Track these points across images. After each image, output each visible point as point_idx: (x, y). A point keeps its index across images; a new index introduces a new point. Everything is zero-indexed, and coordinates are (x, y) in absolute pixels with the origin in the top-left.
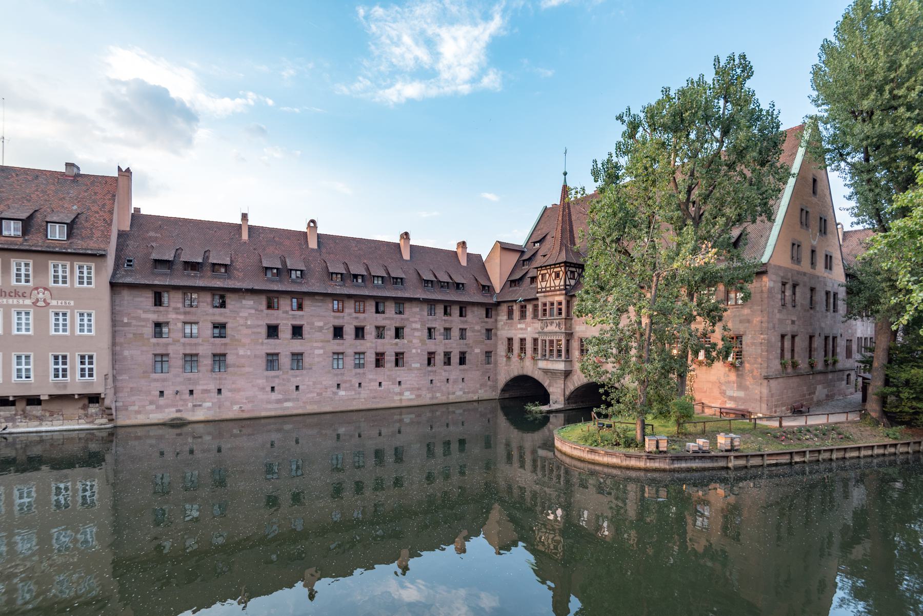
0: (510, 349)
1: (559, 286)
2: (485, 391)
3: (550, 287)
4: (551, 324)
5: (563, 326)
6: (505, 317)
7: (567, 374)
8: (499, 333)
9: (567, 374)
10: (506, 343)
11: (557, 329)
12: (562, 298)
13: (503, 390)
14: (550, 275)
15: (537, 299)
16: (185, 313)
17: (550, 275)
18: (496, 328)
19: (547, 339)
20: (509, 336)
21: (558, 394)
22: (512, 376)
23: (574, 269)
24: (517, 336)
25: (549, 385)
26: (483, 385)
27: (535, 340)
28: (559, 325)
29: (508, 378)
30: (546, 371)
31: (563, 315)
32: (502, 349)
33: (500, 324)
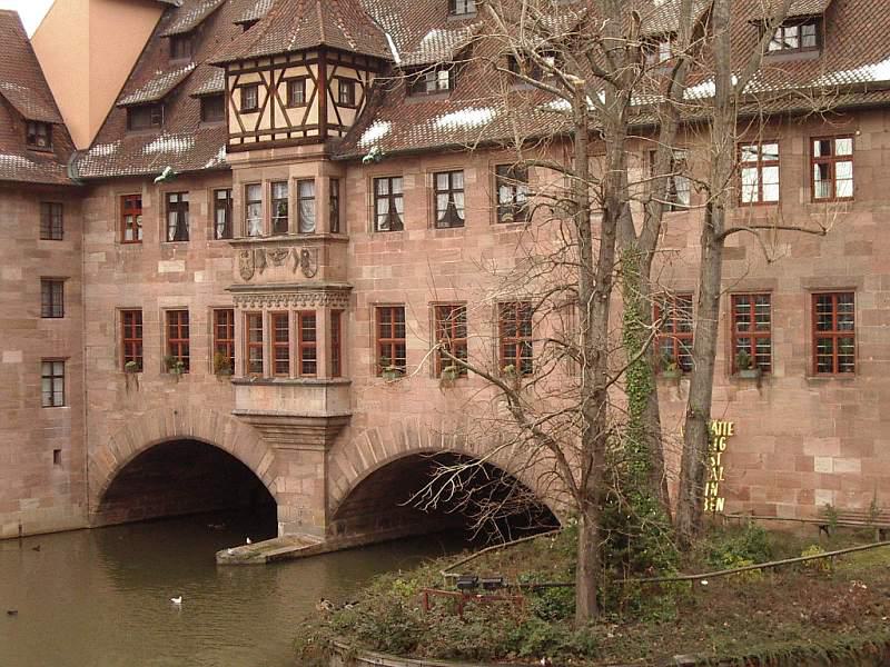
0: (132, 352)
1: (304, 128)
2: (46, 502)
3: (273, 131)
4: (278, 259)
5: (318, 268)
6: (111, 237)
7: (335, 429)
8: (91, 293)
9: (335, 429)
10: (116, 326)
11: (298, 277)
12: (313, 169)
13: (111, 496)
14: (272, 90)
17: (272, 90)
18: (81, 277)
19: (265, 310)
20: (130, 302)
21: (303, 497)
22: (141, 443)
23: (350, 74)
24: (156, 300)
25: (275, 474)
26: (36, 482)
27: (223, 316)
28: (304, 262)
29: (127, 453)
30: (262, 424)
32: (102, 348)
33: (94, 261)
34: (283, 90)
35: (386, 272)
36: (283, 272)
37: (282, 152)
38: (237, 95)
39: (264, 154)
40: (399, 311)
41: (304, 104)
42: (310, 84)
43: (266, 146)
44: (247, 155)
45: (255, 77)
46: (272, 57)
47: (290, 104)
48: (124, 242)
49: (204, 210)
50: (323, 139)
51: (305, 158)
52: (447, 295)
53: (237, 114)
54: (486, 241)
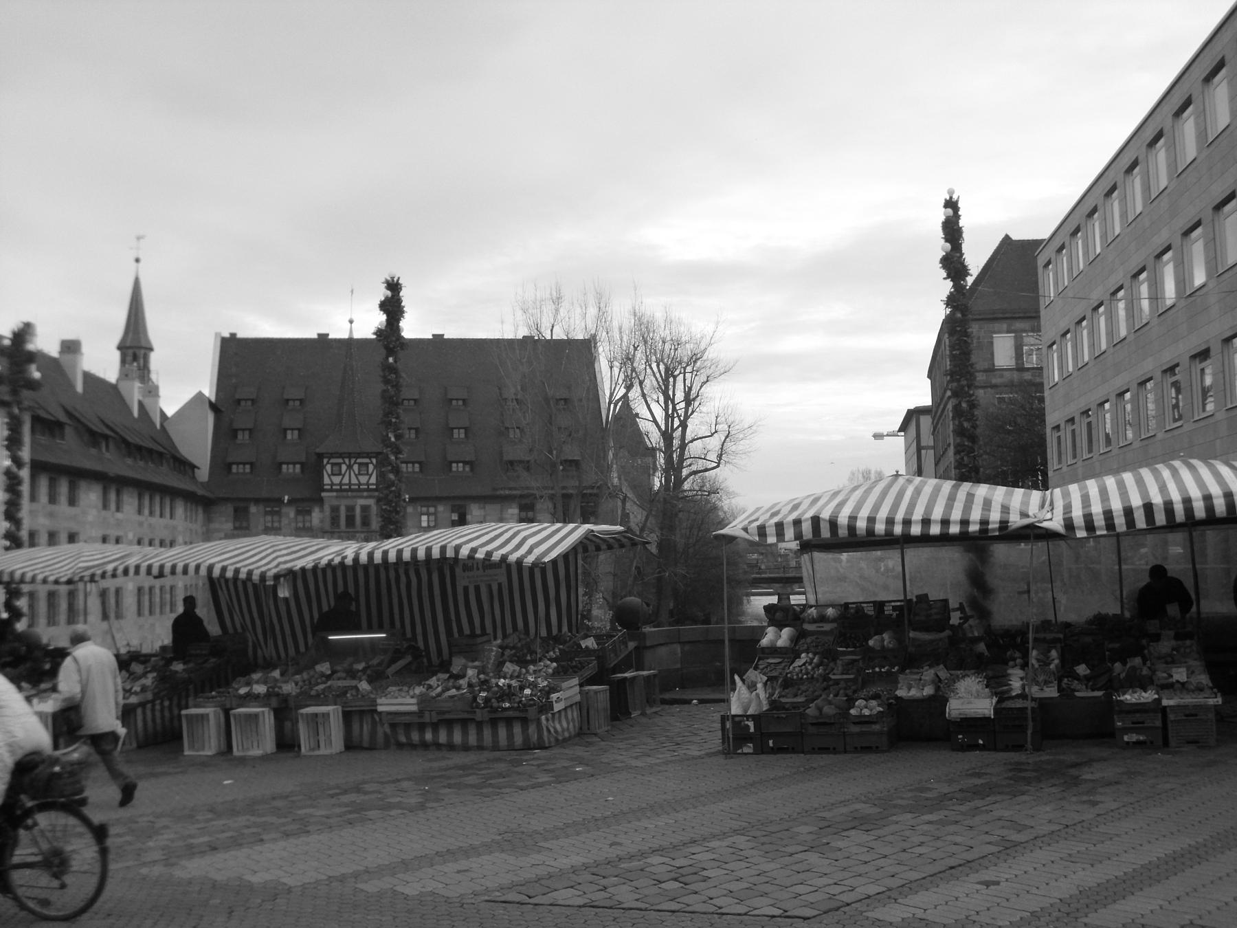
1: (368, 484)
3: (350, 484)
6: (229, 526)
12: (371, 502)
14: (350, 467)
15: (320, 501)
16: (51, 515)
17: (350, 467)
34: (356, 467)
38: (329, 467)
42: (371, 467)
43: (345, 490)
45: (340, 461)
48: (235, 528)
49: (292, 515)
51: (367, 497)
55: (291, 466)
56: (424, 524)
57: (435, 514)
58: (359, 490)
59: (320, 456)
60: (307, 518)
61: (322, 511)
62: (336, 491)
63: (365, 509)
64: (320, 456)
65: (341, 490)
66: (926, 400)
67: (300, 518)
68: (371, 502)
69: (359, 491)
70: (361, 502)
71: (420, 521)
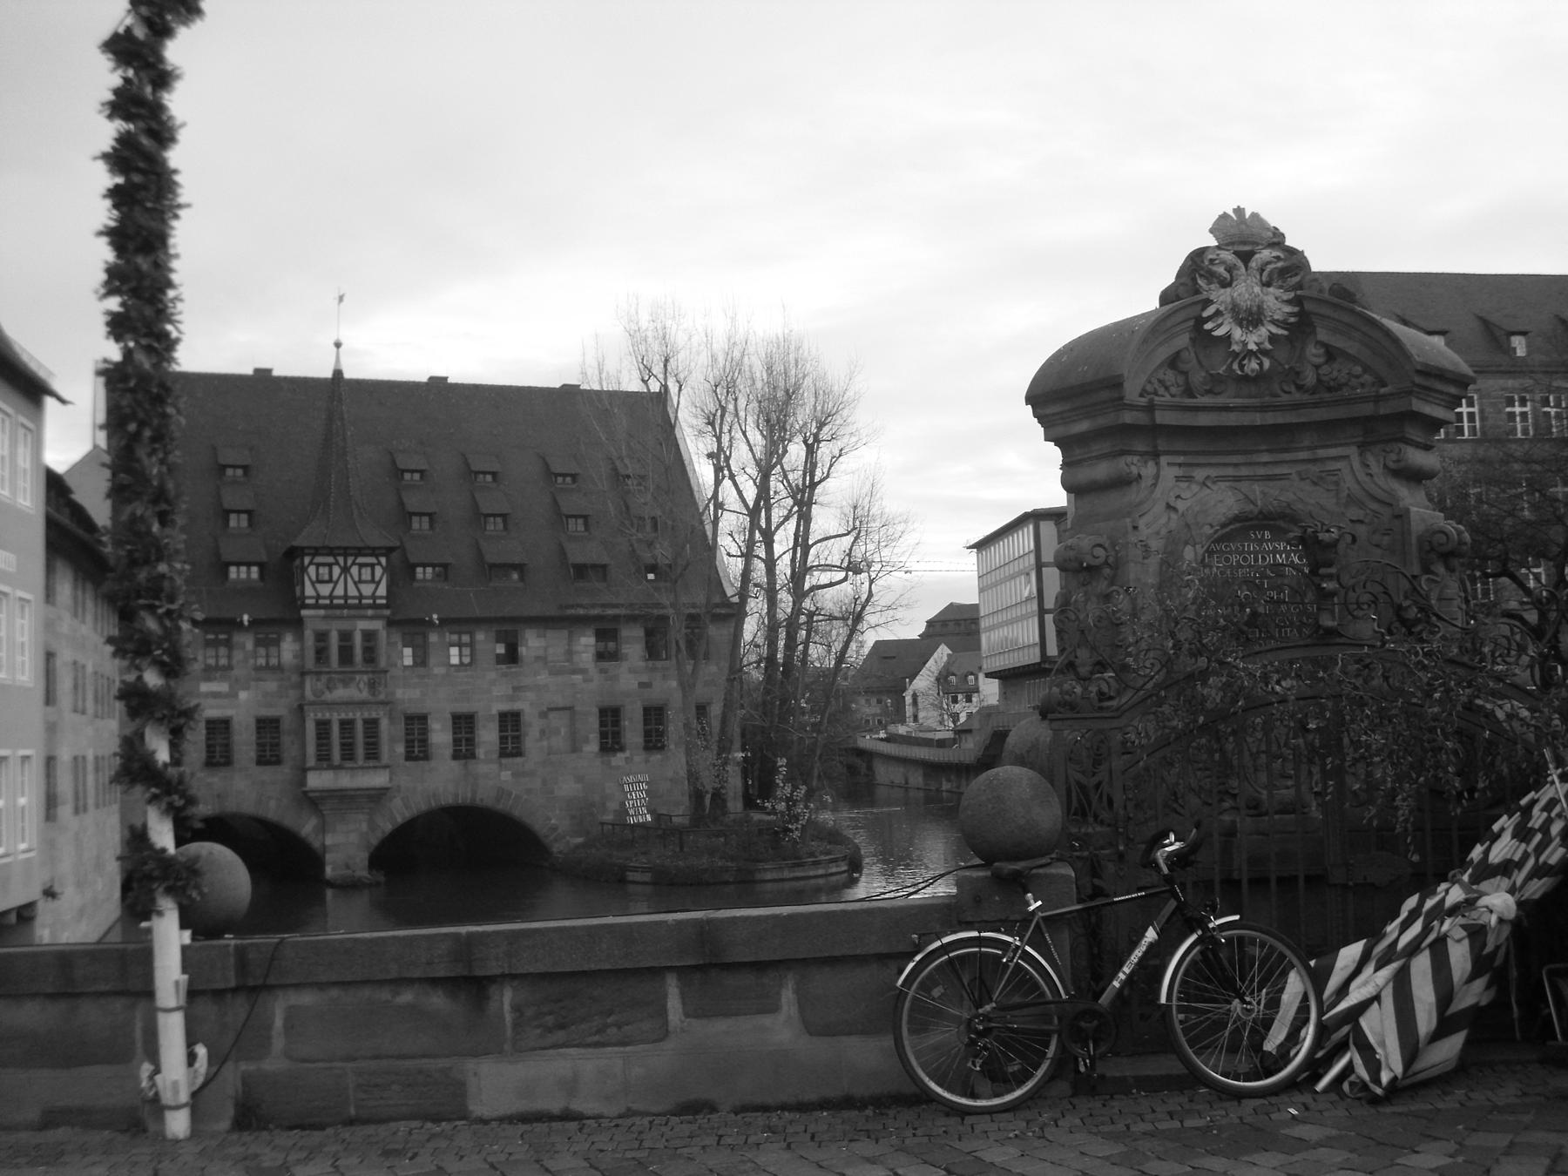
1: (373, 597)
3: (346, 597)
12: (378, 625)
14: (345, 570)
15: (297, 624)
17: (345, 570)
19: (335, 717)
21: (345, 846)
27: (268, 726)
28: (372, 686)
31: (383, 663)
34: (355, 570)
35: (415, 693)
36: (356, 691)
37: (353, 612)
39: (338, 612)
40: (423, 719)
41: (373, 581)
42: (378, 571)
43: (339, 607)
44: (322, 612)
45: (330, 560)
46: (346, 548)
47: (361, 581)
49: (250, 646)
50: (387, 606)
51: (372, 618)
52: (463, 708)
53: (313, 583)
54: (492, 675)
55: (243, 569)
56: (455, 660)
57: (471, 645)
58: (360, 606)
59: (293, 553)
60: (273, 650)
61: (300, 637)
62: (325, 607)
63: (369, 636)
64: (293, 553)
65: (331, 606)
66: (1058, 498)
67: (262, 651)
68: (378, 625)
69: (358, 607)
70: (363, 625)
71: (449, 657)
